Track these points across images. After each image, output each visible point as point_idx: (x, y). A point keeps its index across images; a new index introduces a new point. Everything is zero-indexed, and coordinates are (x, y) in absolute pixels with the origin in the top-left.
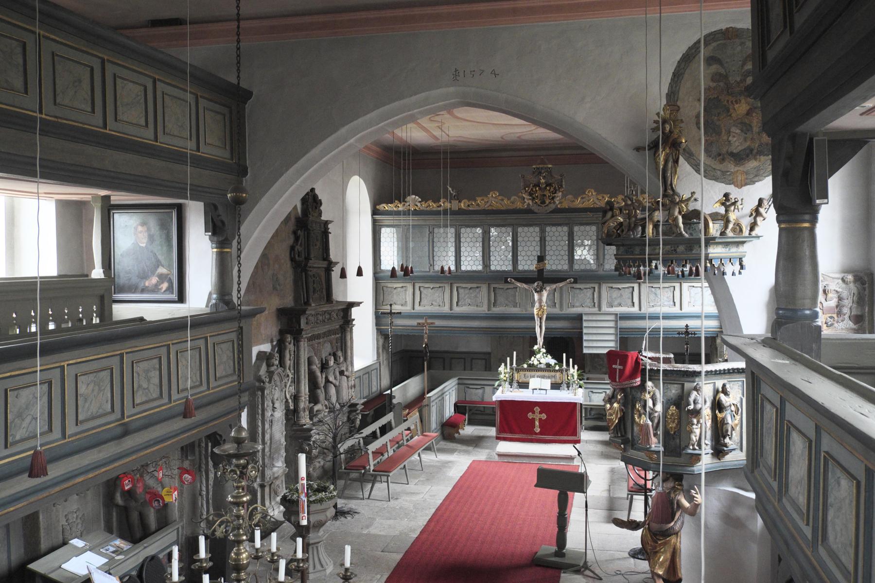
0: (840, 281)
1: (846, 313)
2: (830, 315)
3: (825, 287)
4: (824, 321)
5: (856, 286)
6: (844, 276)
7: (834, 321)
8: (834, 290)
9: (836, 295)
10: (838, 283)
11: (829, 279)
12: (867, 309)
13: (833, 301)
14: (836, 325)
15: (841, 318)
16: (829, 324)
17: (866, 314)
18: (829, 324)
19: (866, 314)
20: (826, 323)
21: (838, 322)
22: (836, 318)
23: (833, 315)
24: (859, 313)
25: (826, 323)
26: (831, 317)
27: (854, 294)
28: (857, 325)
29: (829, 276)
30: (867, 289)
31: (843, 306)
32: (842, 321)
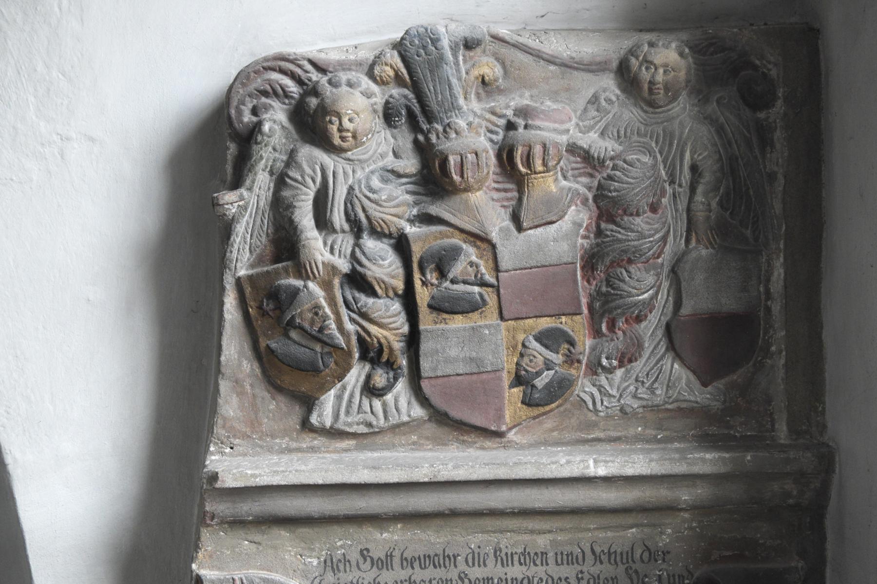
0: (608, 84)
1: (649, 305)
2: (545, 323)
3: (511, 126)
4: (508, 364)
5: (710, 120)
6: (632, 52)
7: (571, 360)
8: (573, 149)
9: (580, 186)
10: (594, 100)
11: (537, 70)
12: (779, 273)
13: (565, 224)
14: (585, 388)
15: (619, 342)
16: (540, 382)
17: (776, 308)
18: (540, 382)
19: (776, 308)
20: (519, 380)
21: (595, 368)
22: (586, 343)
23: (565, 323)
24: (729, 303)
25: (519, 380)
26: (544, 336)
27: (694, 168)
28: (720, 384)
29: (537, 55)
30: (778, 135)
31: (627, 258)
32: (626, 359)
